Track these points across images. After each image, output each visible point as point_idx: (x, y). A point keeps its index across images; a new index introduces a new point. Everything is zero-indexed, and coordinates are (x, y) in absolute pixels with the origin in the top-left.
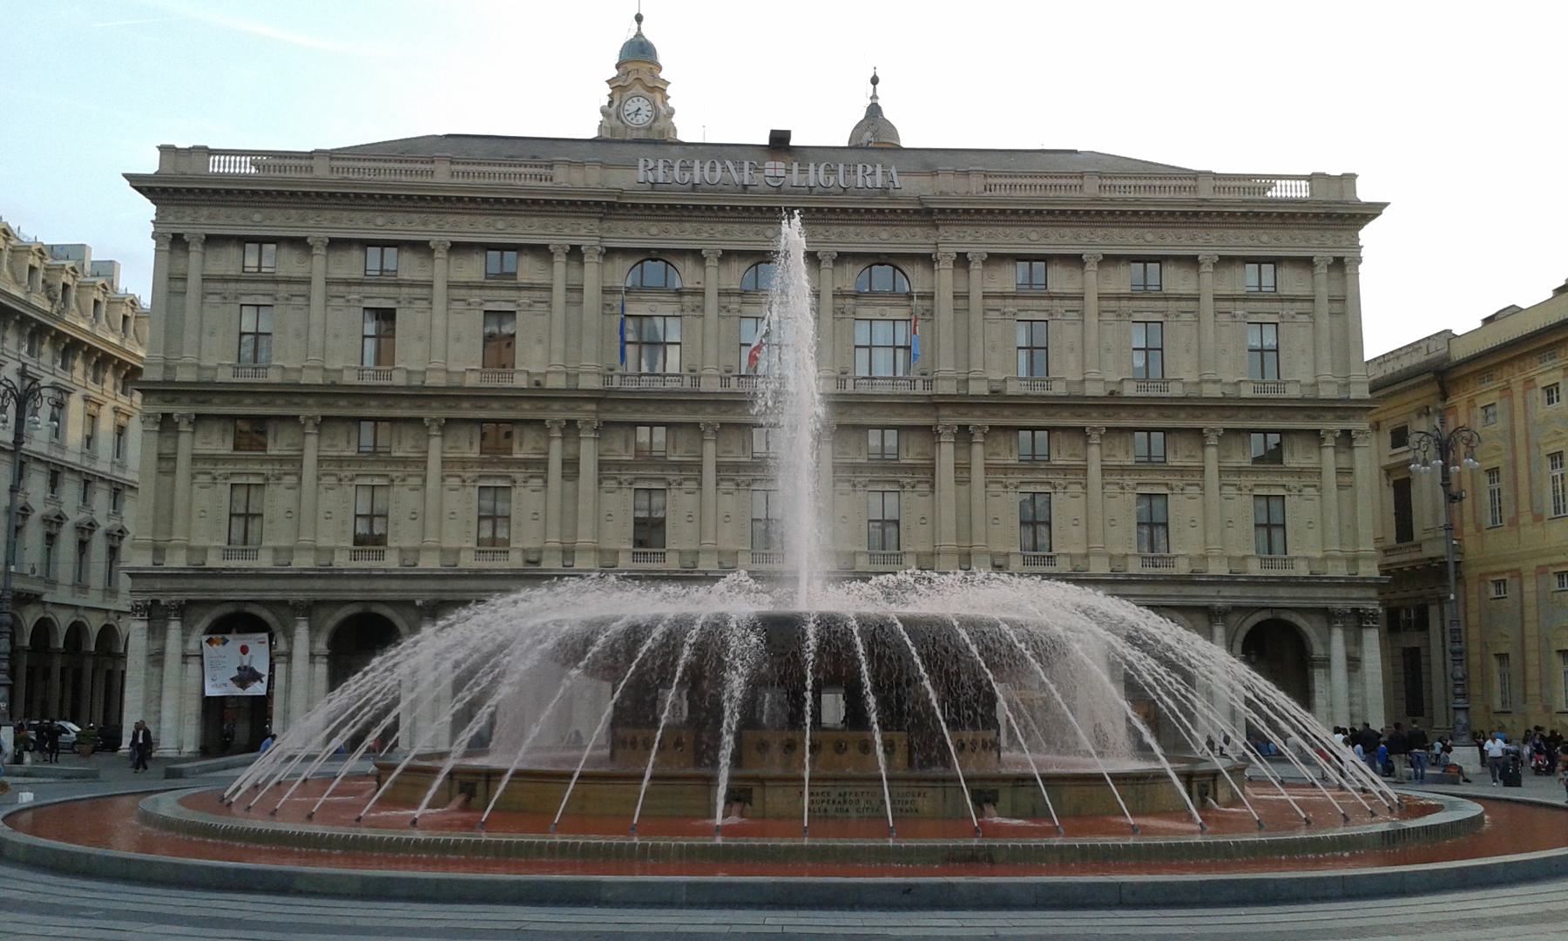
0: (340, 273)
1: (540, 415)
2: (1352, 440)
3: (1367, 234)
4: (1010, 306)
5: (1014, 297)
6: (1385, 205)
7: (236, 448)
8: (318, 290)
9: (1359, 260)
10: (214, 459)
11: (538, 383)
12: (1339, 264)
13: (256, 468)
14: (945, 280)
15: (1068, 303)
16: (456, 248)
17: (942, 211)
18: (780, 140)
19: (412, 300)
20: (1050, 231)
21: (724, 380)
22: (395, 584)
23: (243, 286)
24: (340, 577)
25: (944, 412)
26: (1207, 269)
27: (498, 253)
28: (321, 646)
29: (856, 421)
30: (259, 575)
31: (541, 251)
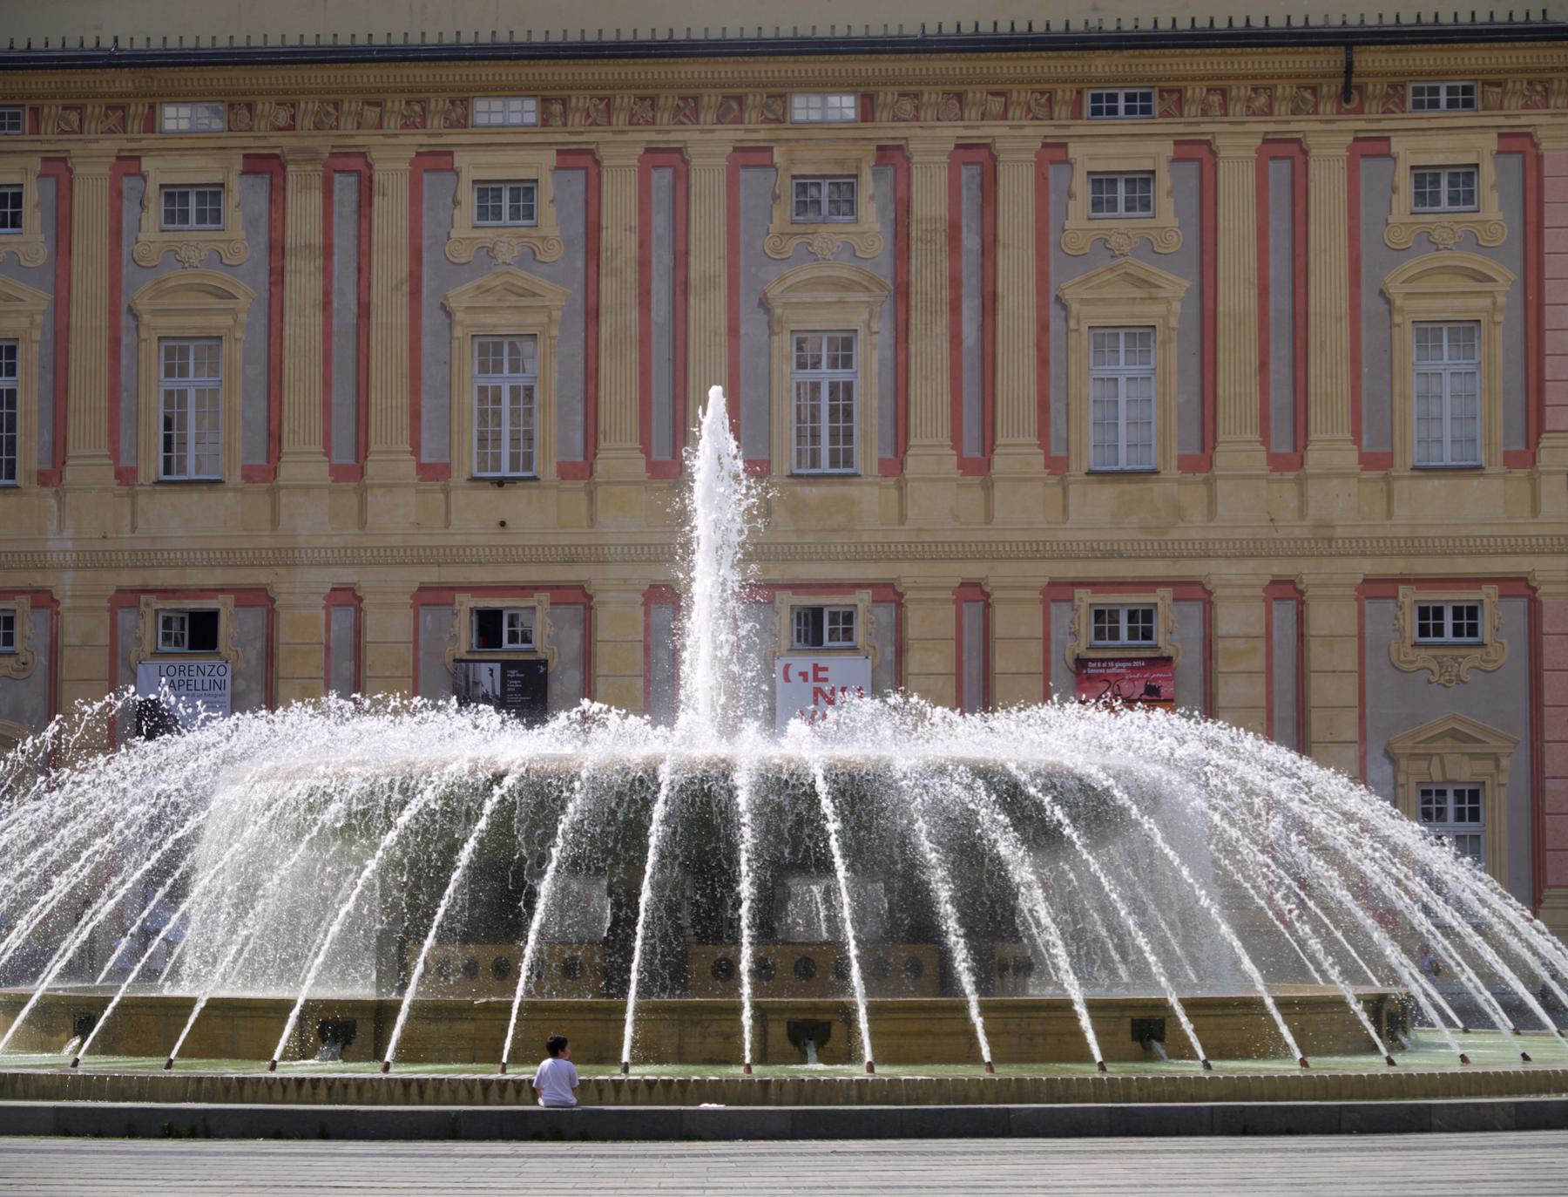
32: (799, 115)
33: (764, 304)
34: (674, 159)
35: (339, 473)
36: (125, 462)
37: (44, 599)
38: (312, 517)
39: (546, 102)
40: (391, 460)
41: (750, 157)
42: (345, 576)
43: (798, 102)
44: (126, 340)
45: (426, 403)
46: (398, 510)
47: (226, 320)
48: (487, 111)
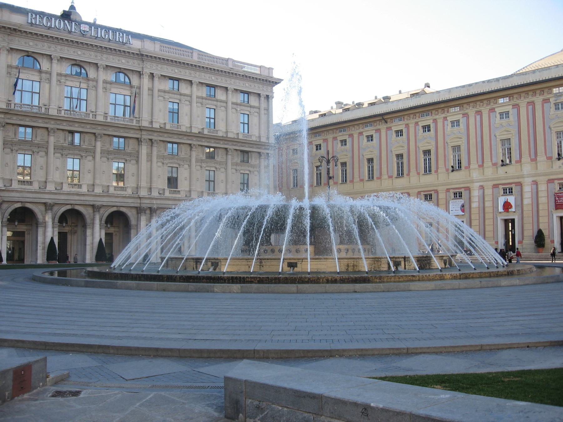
2: (268, 156)
3: (276, 89)
4: (167, 96)
5: (169, 93)
6: (282, 80)
9: (273, 98)
12: (267, 97)
14: (146, 82)
15: (186, 97)
17: (147, 56)
18: (66, 16)
20: (181, 70)
21: (59, 111)
25: (144, 133)
26: (230, 92)
29: (110, 133)
32: (554, 92)
33: (550, 128)
34: (532, 103)
35: (479, 166)
36: (447, 168)
37: (437, 192)
38: (475, 174)
39: (510, 97)
40: (488, 163)
41: (547, 101)
42: (481, 184)
43: (554, 89)
44: (446, 147)
45: (493, 152)
46: (489, 172)
47: (461, 142)
48: (501, 101)
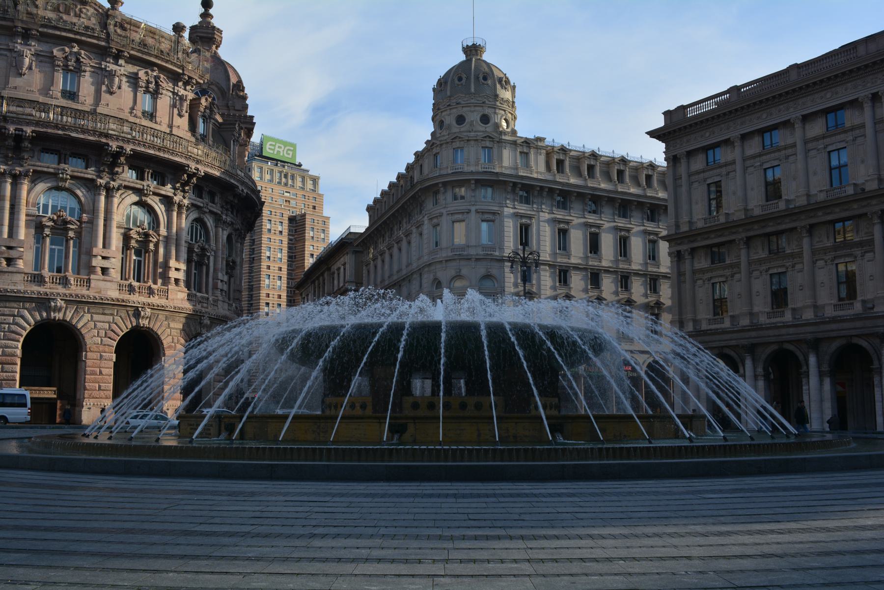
0: (749, 152)
1: (864, 210)
7: (713, 262)
8: (738, 167)
10: (703, 271)
11: (863, 190)
13: (721, 272)
16: (805, 118)
19: (787, 157)
22: (791, 330)
23: (707, 174)
24: (762, 329)
27: (833, 114)
28: (760, 370)
30: (724, 332)
31: (854, 104)
